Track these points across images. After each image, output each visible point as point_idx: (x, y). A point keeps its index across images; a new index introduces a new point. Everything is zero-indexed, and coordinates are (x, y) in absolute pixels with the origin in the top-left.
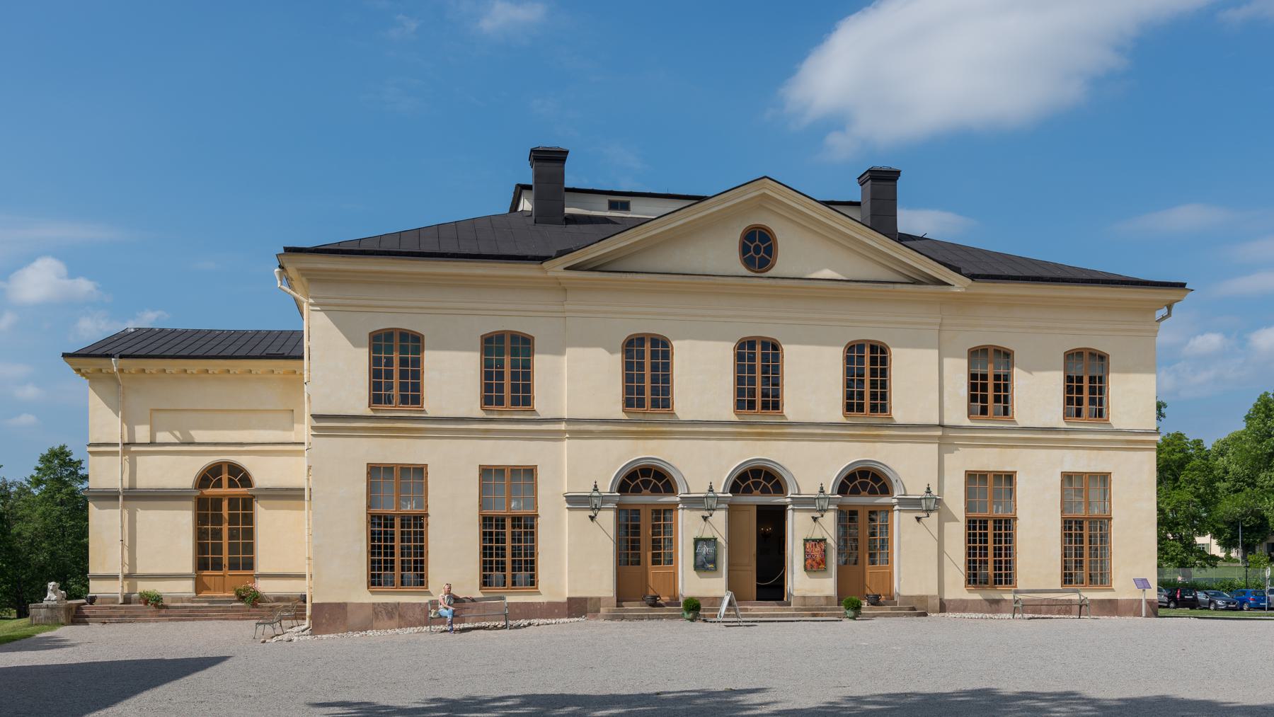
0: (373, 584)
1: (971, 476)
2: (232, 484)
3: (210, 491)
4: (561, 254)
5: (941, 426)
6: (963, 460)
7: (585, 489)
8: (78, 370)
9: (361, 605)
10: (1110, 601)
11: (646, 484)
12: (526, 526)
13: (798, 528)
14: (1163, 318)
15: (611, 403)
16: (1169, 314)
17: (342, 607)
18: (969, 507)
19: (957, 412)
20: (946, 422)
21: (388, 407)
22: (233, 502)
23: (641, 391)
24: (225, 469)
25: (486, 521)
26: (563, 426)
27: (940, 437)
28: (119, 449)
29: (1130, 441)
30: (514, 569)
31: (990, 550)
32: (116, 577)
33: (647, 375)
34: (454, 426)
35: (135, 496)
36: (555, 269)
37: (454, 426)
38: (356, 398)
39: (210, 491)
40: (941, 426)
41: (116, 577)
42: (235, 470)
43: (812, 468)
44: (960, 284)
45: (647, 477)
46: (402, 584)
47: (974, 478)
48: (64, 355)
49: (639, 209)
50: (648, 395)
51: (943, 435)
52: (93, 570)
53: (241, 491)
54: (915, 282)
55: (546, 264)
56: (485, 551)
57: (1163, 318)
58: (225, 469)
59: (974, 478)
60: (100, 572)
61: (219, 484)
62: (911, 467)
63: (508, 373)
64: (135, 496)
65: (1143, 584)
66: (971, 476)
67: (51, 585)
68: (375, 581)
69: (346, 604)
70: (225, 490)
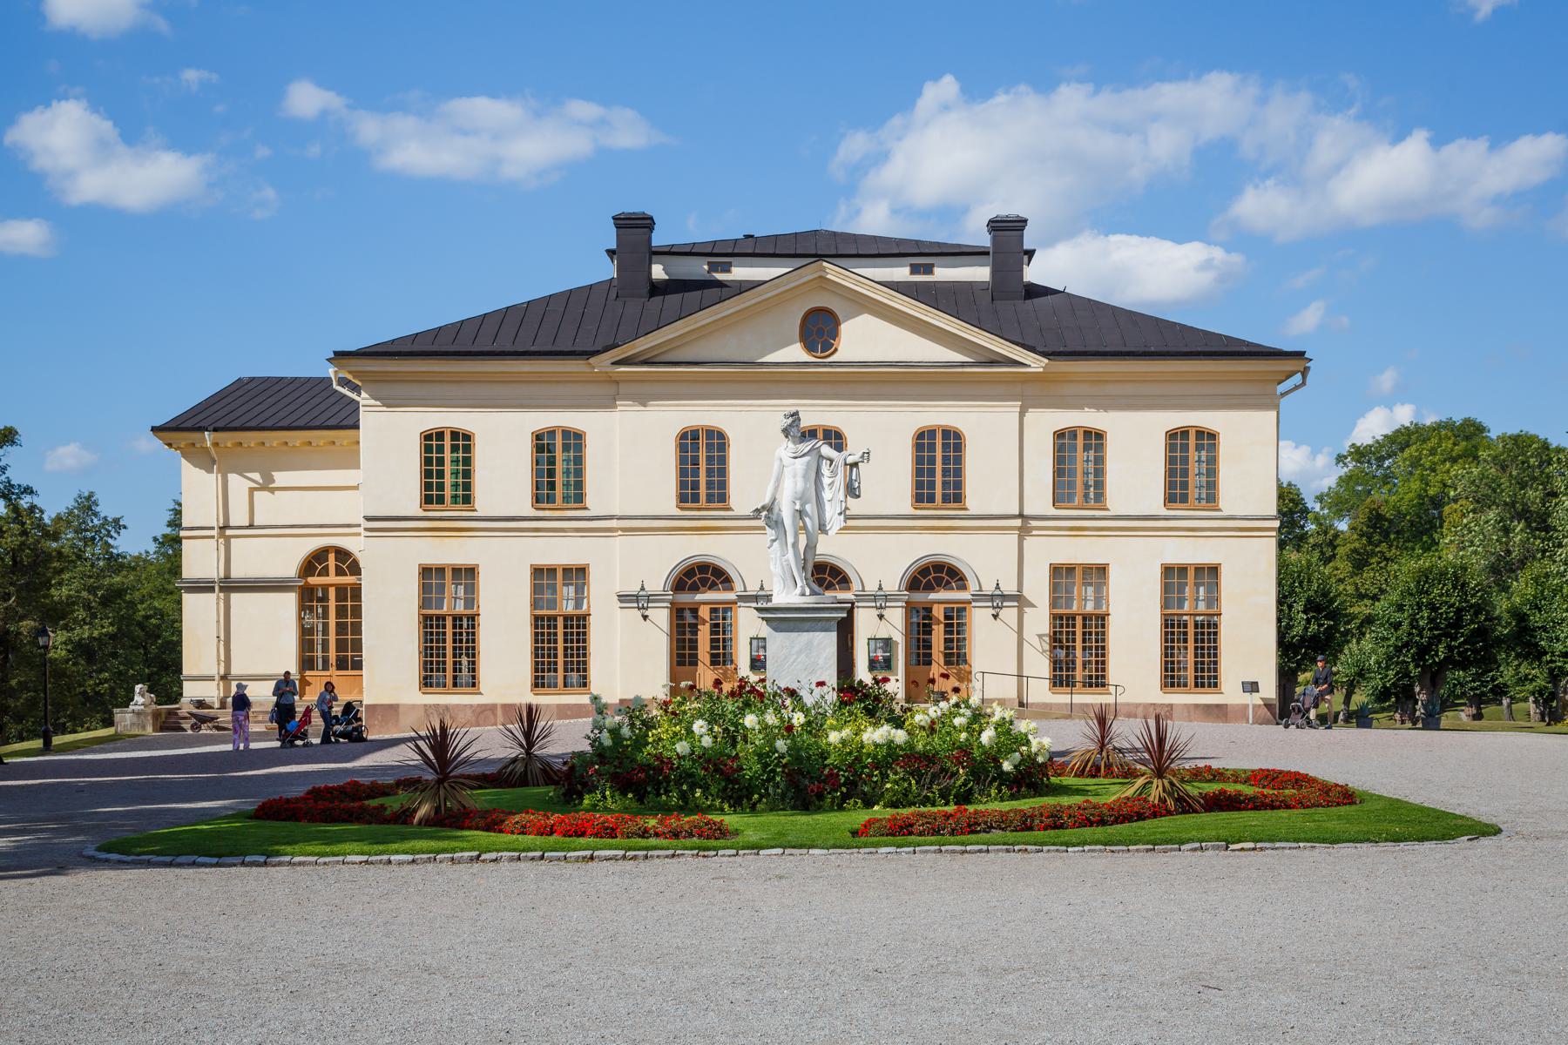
0: (426, 685)
1: (1056, 570)
2: (340, 572)
3: (313, 580)
4: (607, 349)
5: (1021, 516)
6: (1047, 551)
7: (634, 588)
8: (170, 445)
9: (414, 706)
10: (1218, 706)
11: (704, 582)
12: (578, 625)
13: (866, 625)
14: (1297, 387)
15: (664, 497)
16: (1304, 383)
17: (394, 708)
18: (1054, 603)
19: (1040, 500)
20: (1026, 513)
21: (439, 507)
22: (341, 591)
23: (696, 485)
24: (332, 556)
25: (537, 620)
26: (614, 524)
27: (1019, 529)
28: (214, 533)
29: (1244, 527)
30: (566, 670)
31: (1077, 645)
32: (211, 678)
33: (702, 467)
34: (506, 524)
35: (230, 586)
36: (602, 363)
37: (506, 524)
38: (407, 498)
39: (313, 580)
40: (1021, 516)
41: (211, 678)
42: (342, 554)
43: (880, 563)
44: (1036, 363)
45: (701, 574)
46: (455, 685)
47: (1061, 573)
48: (154, 429)
49: (740, 272)
50: (703, 490)
51: (1025, 524)
52: (186, 671)
53: (349, 579)
54: (992, 363)
55: (592, 360)
56: (537, 652)
57: (1297, 387)
58: (332, 556)
59: (1061, 573)
60: (195, 673)
61: (325, 572)
62: (985, 559)
63: (558, 471)
64: (230, 586)
65: (1252, 687)
66: (1056, 570)
67: (138, 688)
68: (426, 683)
69: (397, 706)
70: (332, 578)
